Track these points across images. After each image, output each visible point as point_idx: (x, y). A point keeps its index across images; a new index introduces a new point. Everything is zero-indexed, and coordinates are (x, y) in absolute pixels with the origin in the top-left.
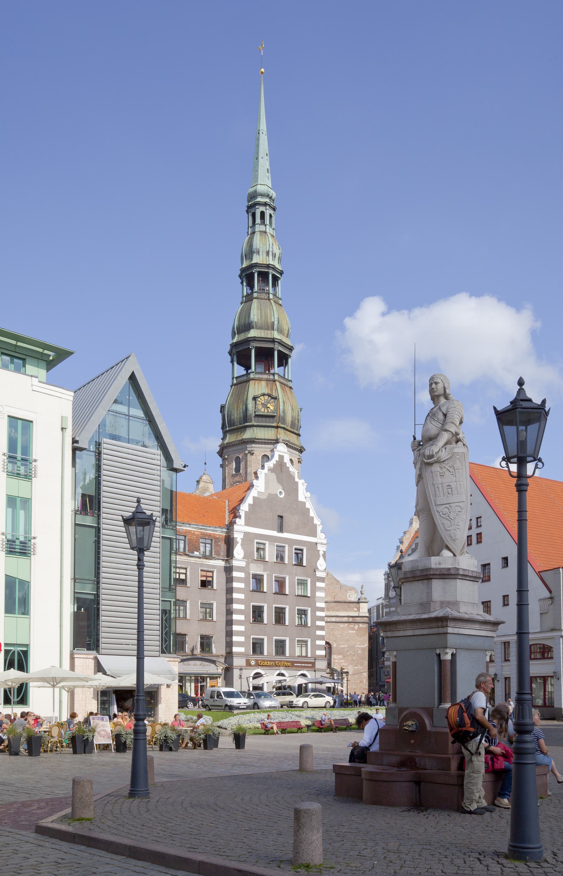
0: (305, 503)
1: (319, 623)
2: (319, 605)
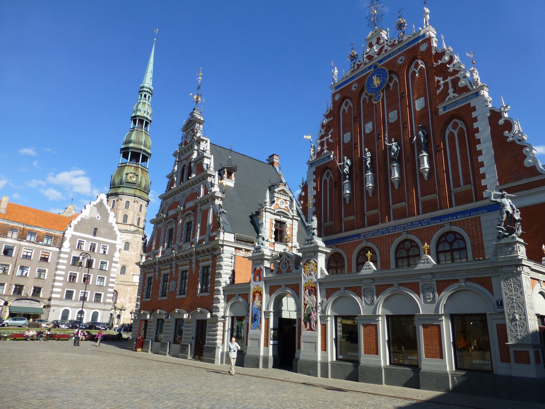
1: (110, 285)
2: (112, 275)
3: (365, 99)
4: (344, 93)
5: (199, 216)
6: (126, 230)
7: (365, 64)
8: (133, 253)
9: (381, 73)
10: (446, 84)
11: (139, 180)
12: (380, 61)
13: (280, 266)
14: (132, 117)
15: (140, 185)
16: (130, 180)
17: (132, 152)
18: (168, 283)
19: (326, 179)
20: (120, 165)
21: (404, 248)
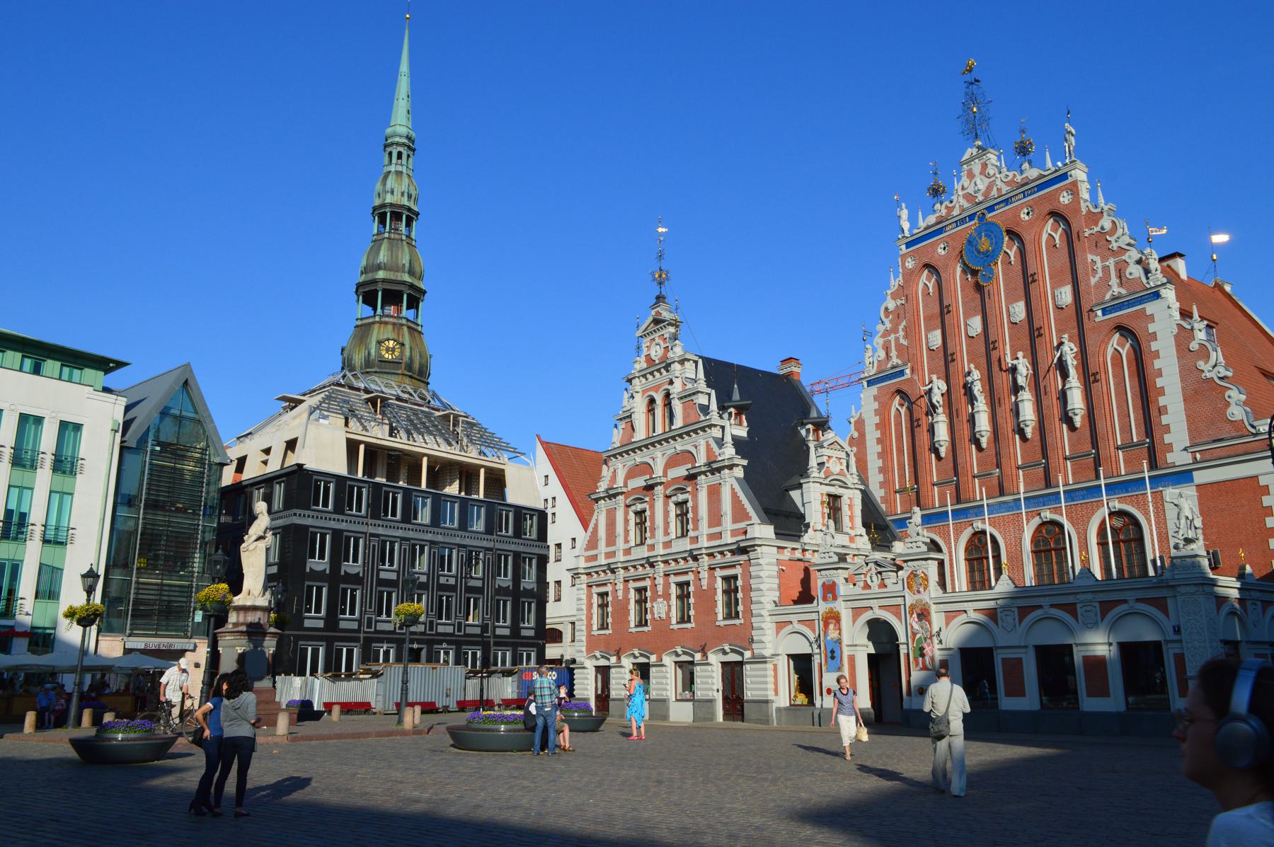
7: (963, 210)
10: (1106, 269)
11: (407, 353)
14: (375, 209)
15: (409, 367)
16: (388, 356)
17: (384, 291)
18: (648, 605)
20: (359, 323)
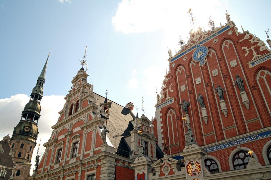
0: (11, 156)
3: (193, 65)
4: (176, 63)
5: (84, 136)
6: (20, 162)
7: (191, 45)
8: (22, 178)
9: (203, 49)
10: (251, 51)
12: (201, 43)
13: (162, 170)
15: (31, 134)
19: (169, 116)
21: (239, 158)
